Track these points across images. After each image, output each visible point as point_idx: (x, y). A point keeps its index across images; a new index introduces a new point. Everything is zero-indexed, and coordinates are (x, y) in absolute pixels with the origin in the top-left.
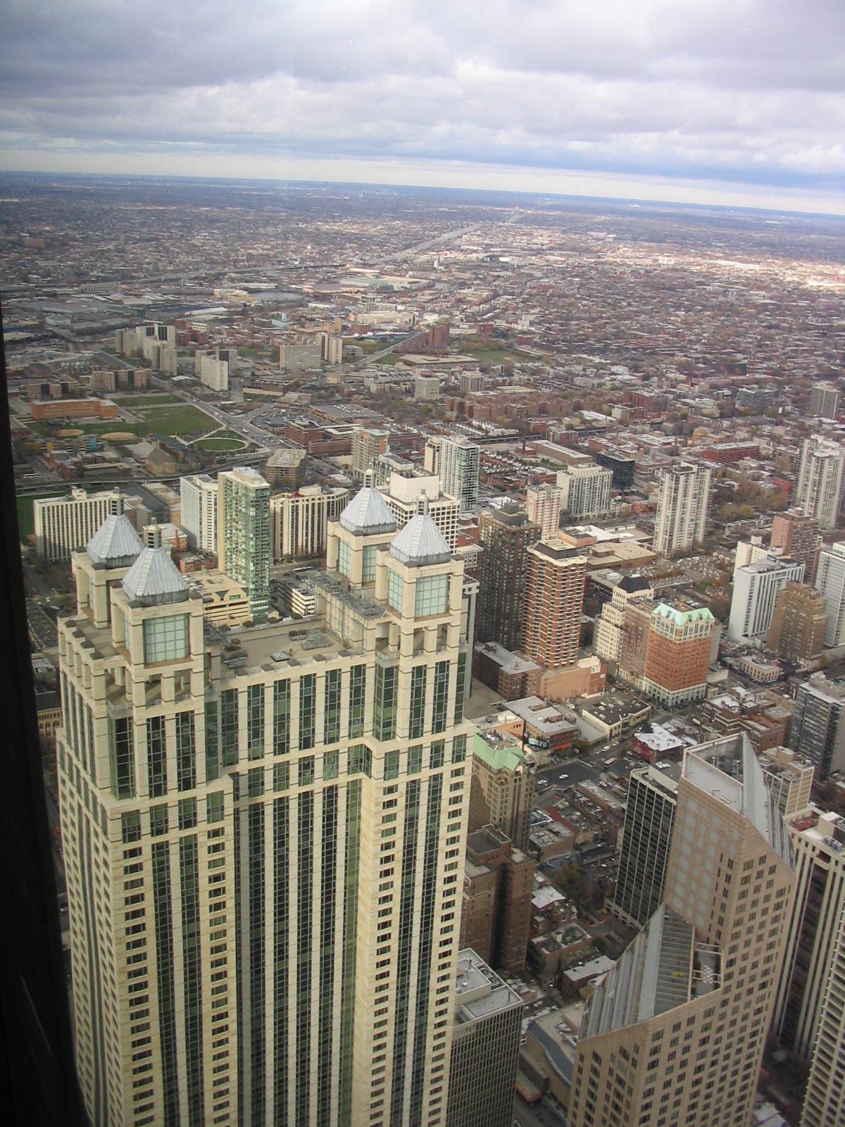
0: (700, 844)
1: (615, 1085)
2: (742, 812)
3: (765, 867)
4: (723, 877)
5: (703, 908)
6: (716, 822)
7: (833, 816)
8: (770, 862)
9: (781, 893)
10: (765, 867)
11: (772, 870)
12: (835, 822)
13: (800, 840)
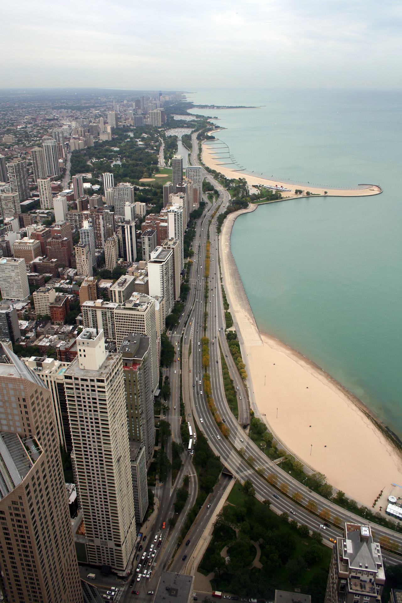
0: (6, 398)
1: (15, 518)
2: (21, 377)
3: (38, 394)
4: (23, 407)
5: (18, 424)
6: (10, 386)
7: (33, 358)
8: (39, 392)
9: (47, 401)
10: (38, 394)
11: (41, 394)
12: (35, 360)
13: (43, 376)
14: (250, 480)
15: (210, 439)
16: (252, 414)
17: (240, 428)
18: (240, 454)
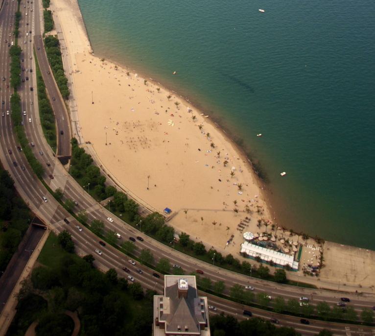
14: (68, 230)
15: (18, 180)
16: (75, 142)
17: (57, 163)
18: (58, 196)
